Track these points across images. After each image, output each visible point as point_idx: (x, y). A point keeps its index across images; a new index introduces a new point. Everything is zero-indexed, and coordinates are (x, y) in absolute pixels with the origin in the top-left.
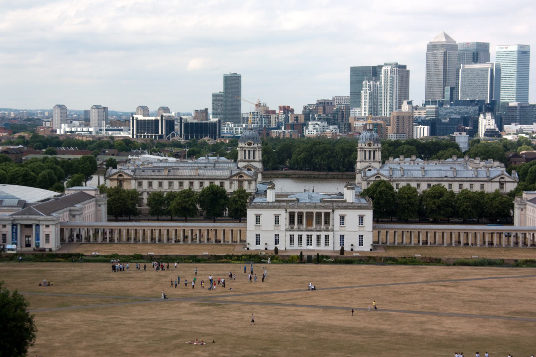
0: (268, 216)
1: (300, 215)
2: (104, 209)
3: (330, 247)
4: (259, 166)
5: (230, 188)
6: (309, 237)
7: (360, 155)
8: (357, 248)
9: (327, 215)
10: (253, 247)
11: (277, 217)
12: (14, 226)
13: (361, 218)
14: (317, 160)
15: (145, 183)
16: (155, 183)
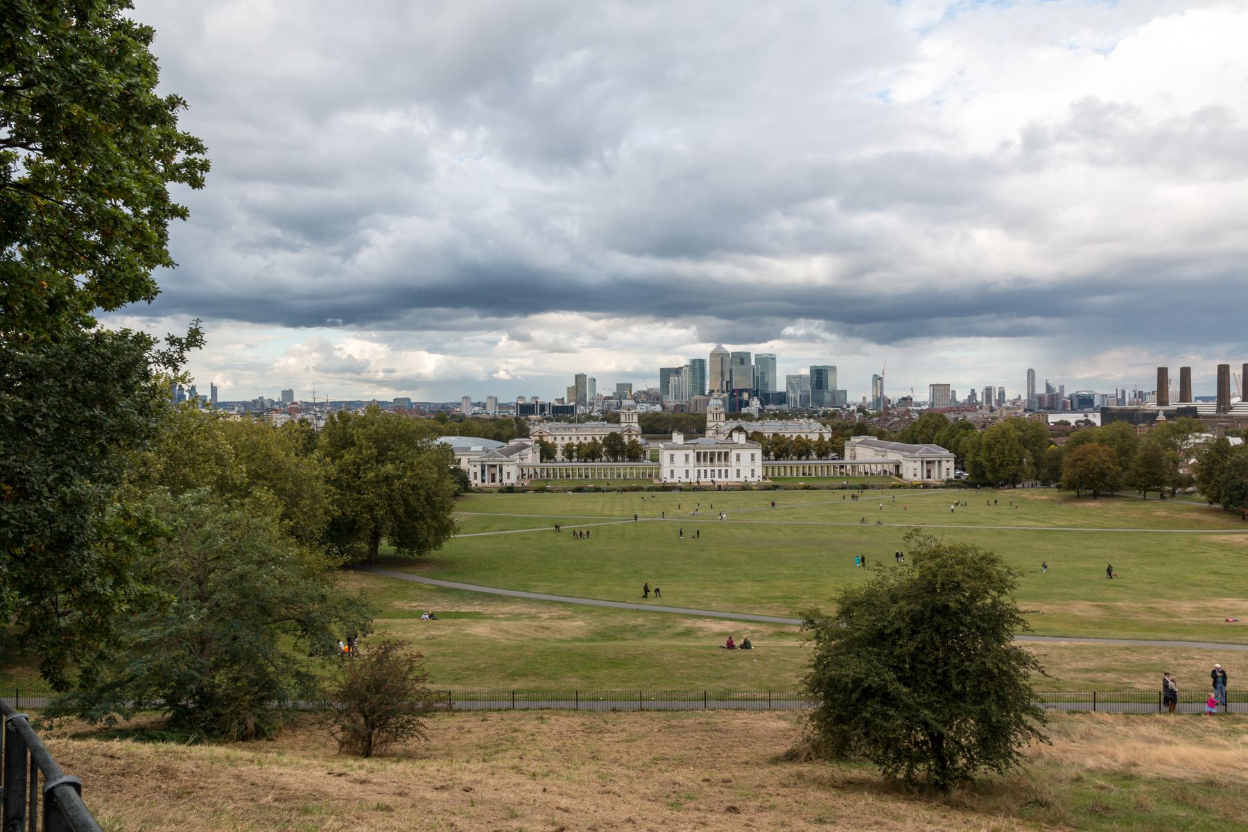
0: (679, 455)
1: (705, 454)
2: (538, 454)
3: (729, 479)
4: (637, 425)
5: (626, 439)
6: (713, 471)
7: (710, 417)
8: (750, 479)
9: (726, 454)
10: (669, 480)
11: (687, 456)
12: (483, 466)
13: (753, 455)
14: (657, 426)
15: (559, 438)
16: (566, 438)
